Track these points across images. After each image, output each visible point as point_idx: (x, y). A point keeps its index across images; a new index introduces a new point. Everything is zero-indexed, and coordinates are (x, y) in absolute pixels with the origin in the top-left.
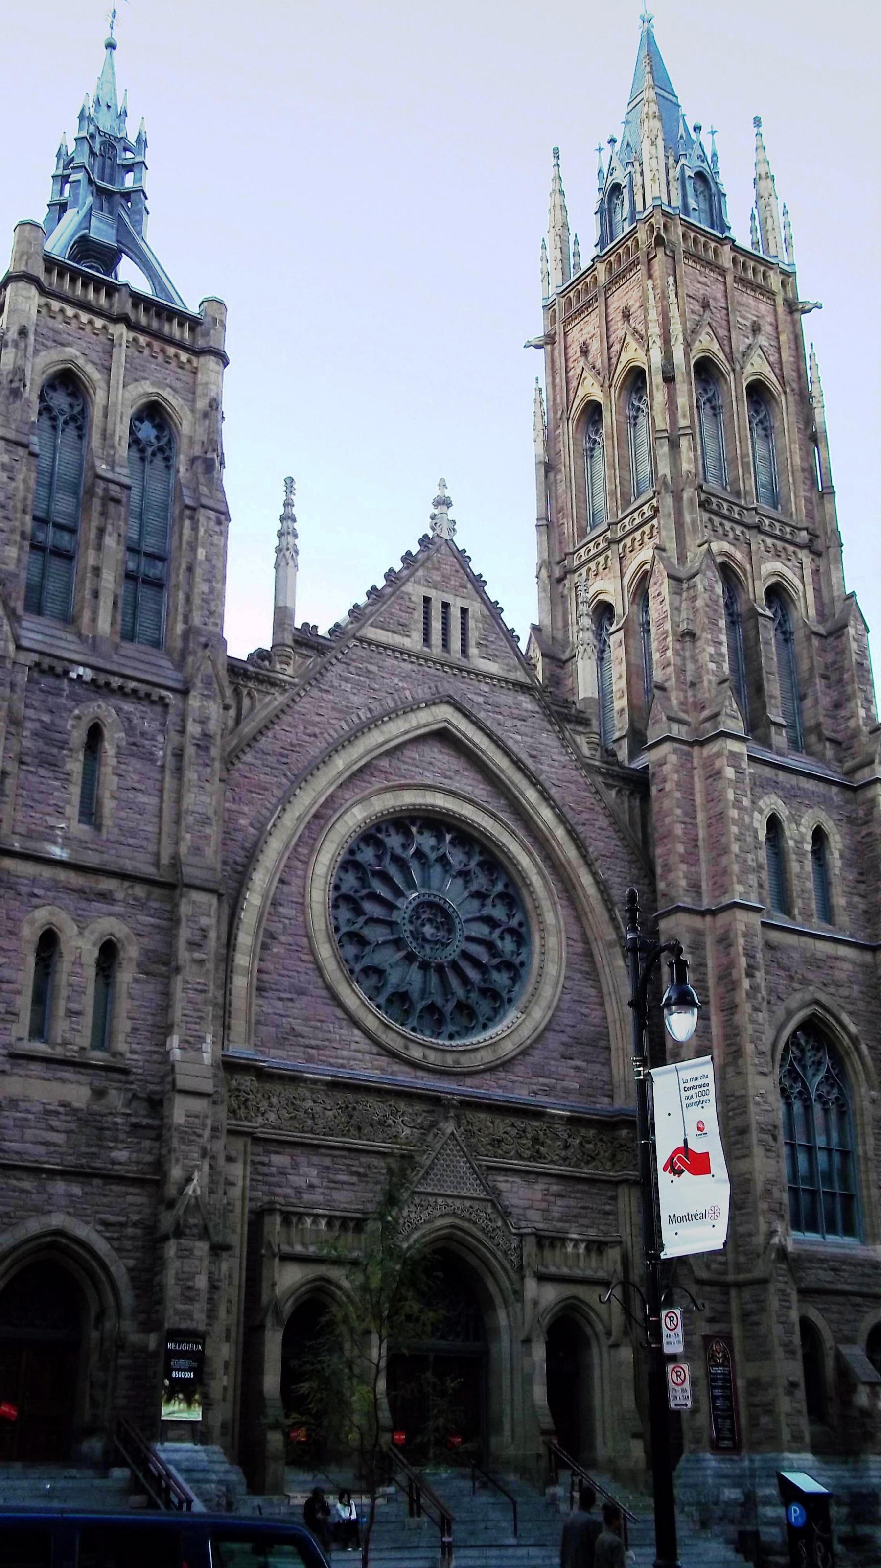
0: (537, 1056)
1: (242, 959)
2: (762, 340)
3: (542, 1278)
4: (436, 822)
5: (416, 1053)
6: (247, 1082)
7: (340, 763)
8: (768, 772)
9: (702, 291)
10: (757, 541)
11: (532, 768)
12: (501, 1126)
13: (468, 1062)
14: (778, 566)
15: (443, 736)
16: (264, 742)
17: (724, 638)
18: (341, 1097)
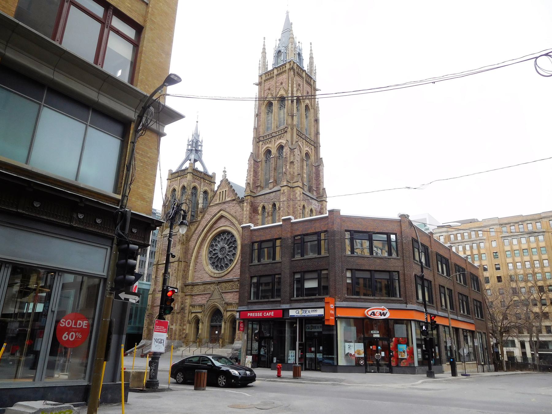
0: (234, 270)
1: (191, 268)
2: (284, 85)
3: (227, 311)
4: (224, 232)
5: (215, 275)
6: (190, 287)
7: (205, 230)
8: (263, 196)
9: (268, 86)
10: (273, 139)
11: (234, 214)
12: (227, 285)
13: (223, 274)
14: (280, 141)
15: (222, 217)
16: (197, 232)
17: (252, 173)
18: (204, 286)
